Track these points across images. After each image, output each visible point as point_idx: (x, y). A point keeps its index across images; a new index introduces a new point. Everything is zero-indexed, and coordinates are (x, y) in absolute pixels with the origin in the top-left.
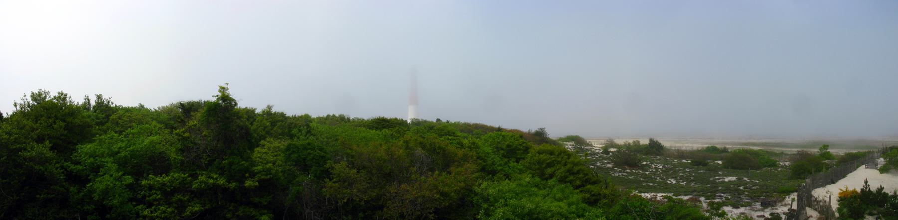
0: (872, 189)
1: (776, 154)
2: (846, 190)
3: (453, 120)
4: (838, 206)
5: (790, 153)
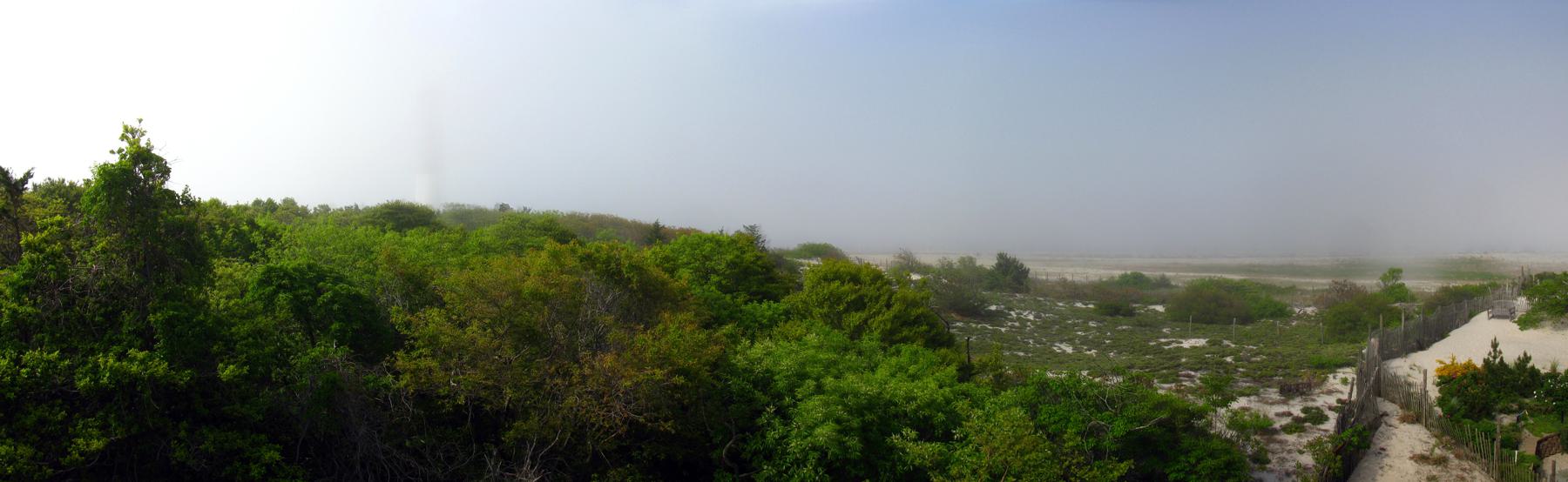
0: (1506, 361)
2: (1453, 364)
4: (1438, 395)
5: (1310, 288)
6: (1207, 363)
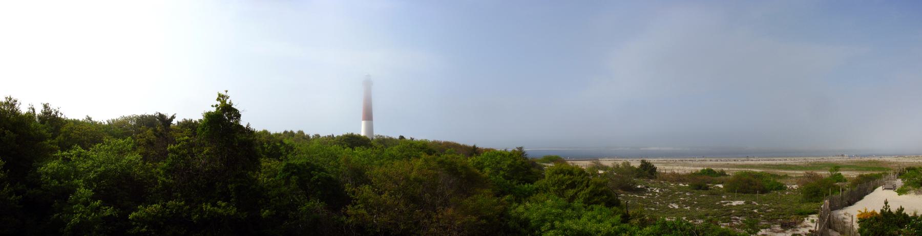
0: (892, 210)
1: (780, 177)
2: (865, 212)
4: (859, 227)
5: (794, 176)
6: (744, 213)
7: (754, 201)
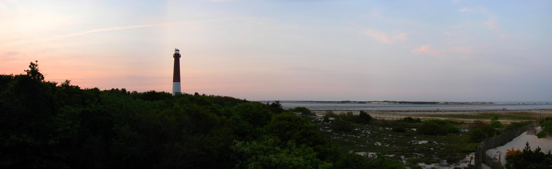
0: (532, 150)
2: (512, 151)
3: (208, 94)
4: (506, 163)
7: (434, 141)
